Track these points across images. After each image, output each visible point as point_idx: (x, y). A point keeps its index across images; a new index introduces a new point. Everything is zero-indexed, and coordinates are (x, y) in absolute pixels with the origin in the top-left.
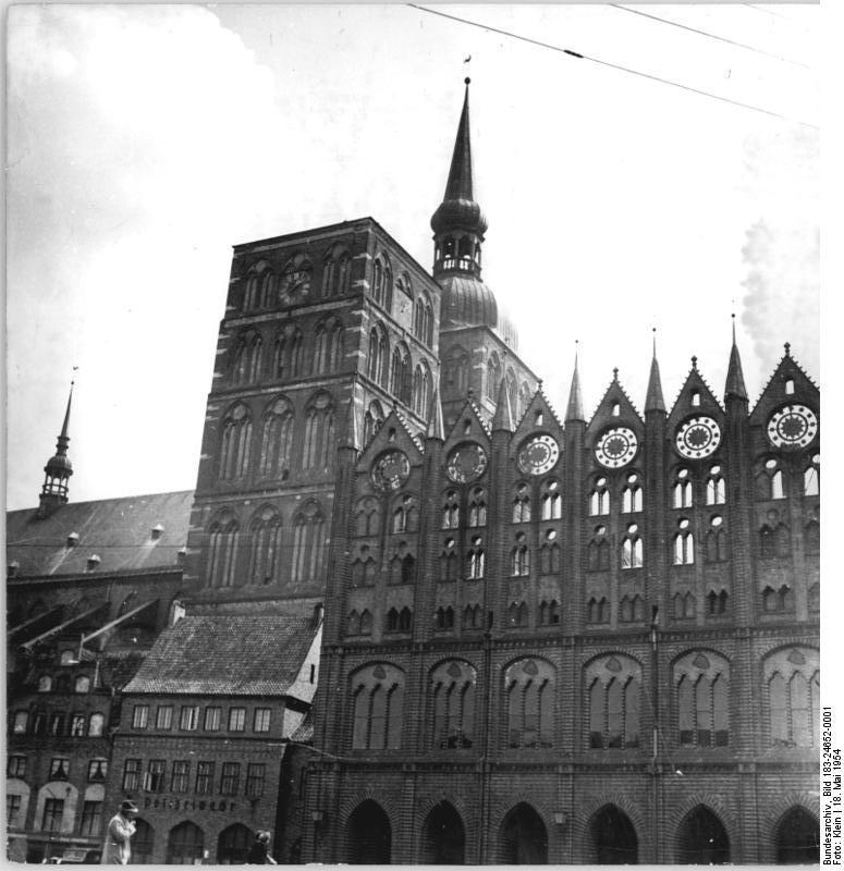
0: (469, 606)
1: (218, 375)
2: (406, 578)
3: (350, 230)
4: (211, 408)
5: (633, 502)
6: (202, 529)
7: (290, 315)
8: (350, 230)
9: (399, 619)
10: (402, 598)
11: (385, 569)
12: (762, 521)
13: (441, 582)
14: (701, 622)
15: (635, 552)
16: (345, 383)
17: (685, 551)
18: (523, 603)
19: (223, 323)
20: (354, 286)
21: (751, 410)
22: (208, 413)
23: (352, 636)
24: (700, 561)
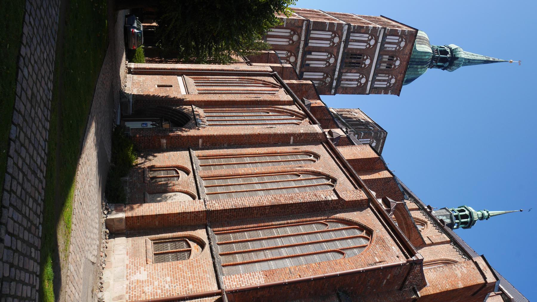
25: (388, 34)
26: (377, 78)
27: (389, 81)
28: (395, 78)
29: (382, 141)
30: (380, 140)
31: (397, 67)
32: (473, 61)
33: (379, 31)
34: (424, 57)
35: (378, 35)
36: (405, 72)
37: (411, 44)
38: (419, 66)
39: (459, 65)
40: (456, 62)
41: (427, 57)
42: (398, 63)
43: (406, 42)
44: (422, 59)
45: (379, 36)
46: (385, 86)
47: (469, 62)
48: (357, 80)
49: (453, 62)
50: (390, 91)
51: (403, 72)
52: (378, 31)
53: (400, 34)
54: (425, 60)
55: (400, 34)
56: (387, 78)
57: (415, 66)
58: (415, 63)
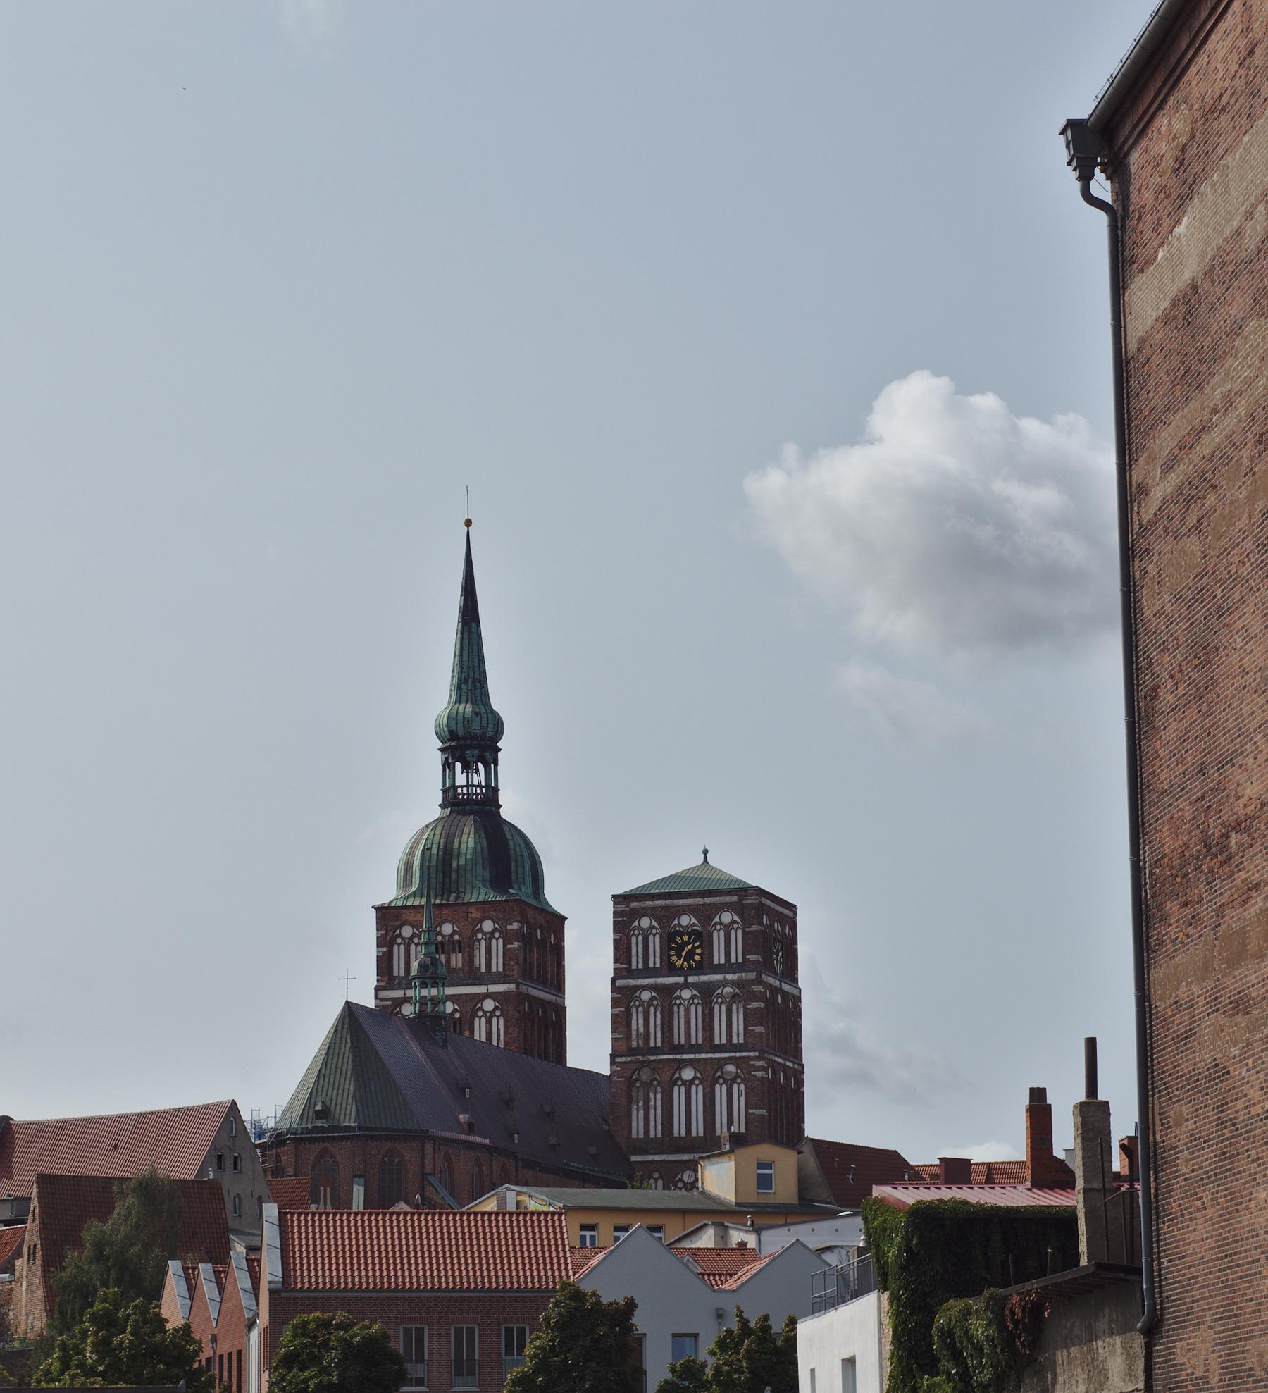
7: (686, 980)
19: (613, 981)
25: (386, 978)
26: (483, 969)
27: (489, 937)
28: (481, 921)
29: (634, 904)
30: (632, 909)
31: (456, 928)
32: (465, 669)
33: (382, 1003)
34: (434, 863)
35: (390, 1003)
36: (464, 904)
37: (404, 911)
38: (454, 864)
39: (466, 722)
40: (461, 733)
41: (434, 851)
42: (447, 929)
43: (400, 927)
44: (437, 865)
45: (392, 999)
46: (501, 941)
47: (466, 681)
48: (489, 1022)
49: (465, 738)
50: (509, 927)
51: (464, 908)
52: (383, 1006)
53: (385, 949)
54: (441, 853)
55: (385, 949)
56: (483, 942)
57: (454, 876)
58: (447, 880)
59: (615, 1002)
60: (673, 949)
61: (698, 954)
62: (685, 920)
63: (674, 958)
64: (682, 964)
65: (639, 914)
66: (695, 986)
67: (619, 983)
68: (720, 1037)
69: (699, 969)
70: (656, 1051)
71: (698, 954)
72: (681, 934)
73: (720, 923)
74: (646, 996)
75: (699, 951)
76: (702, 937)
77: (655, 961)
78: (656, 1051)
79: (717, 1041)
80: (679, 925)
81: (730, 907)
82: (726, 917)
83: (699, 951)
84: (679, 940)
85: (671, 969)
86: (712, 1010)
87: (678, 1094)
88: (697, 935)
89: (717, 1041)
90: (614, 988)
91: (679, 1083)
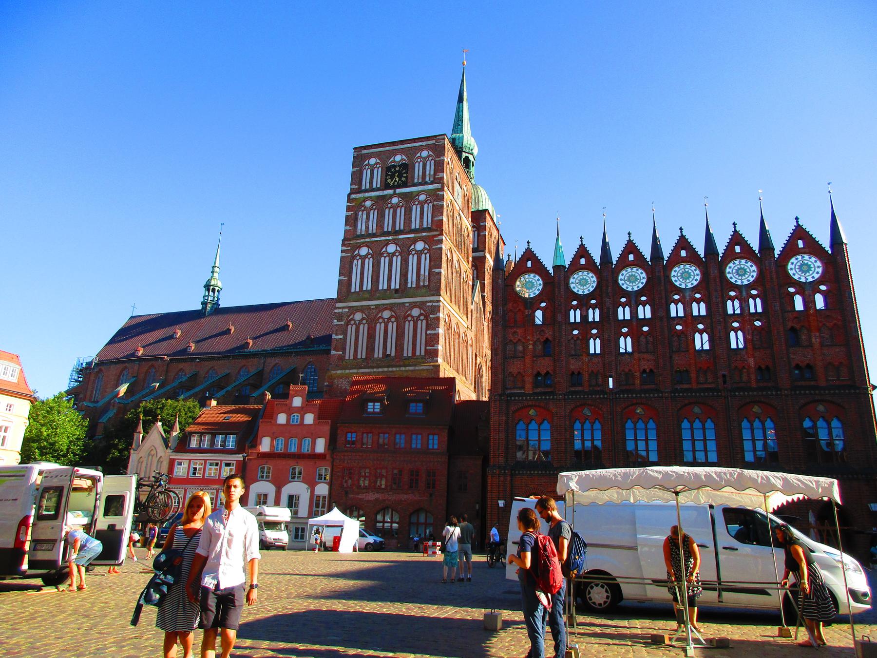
0: (592, 371)
1: (348, 228)
2: (546, 353)
3: (433, 142)
4: (345, 248)
5: (700, 309)
6: (343, 323)
7: (395, 192)
8: (433, 142)
9: (542, 379)
10: (544, 365)
11: (531, 347)
12: (790, 325)
13: (572, 355)
14: (754, 385)
15: (701, 342)
16: (439, 235)
17: (736, 340)
18: (630, 370)
19: (349, 195)
20: (436, 177)
21: (776, 256)
22: (342, 251)
23: (511, 389)
24: (749, 346)
59: (348, 209)
60: (389, 175)
61: (404, 177)
62: (398, 158)
63: (389, 181)
64: (394, 183)
65: (369, 156)
66: (400, 195)
67: (353, 196)
68: (415, 224)
69: (405, 185)
70: (374, 235)
71: (404, 177)
72: (394, 166)
73: (420, 157)
74: (368, 203)
75: (405, 175)
76: (406, 168)
77: (377, 182)
78: (374, 235)
79: (413, 227)
80: (394, 161)
81: (428, 147)
82: (425, 154)
83: (405, 175)
84: (393, 170)
85: (387, 186)
86: (411, 210)
87: (384, 262)
88: (404, 166)
89: (413, 227)
90: (349, 200)
91: (385, 255)
